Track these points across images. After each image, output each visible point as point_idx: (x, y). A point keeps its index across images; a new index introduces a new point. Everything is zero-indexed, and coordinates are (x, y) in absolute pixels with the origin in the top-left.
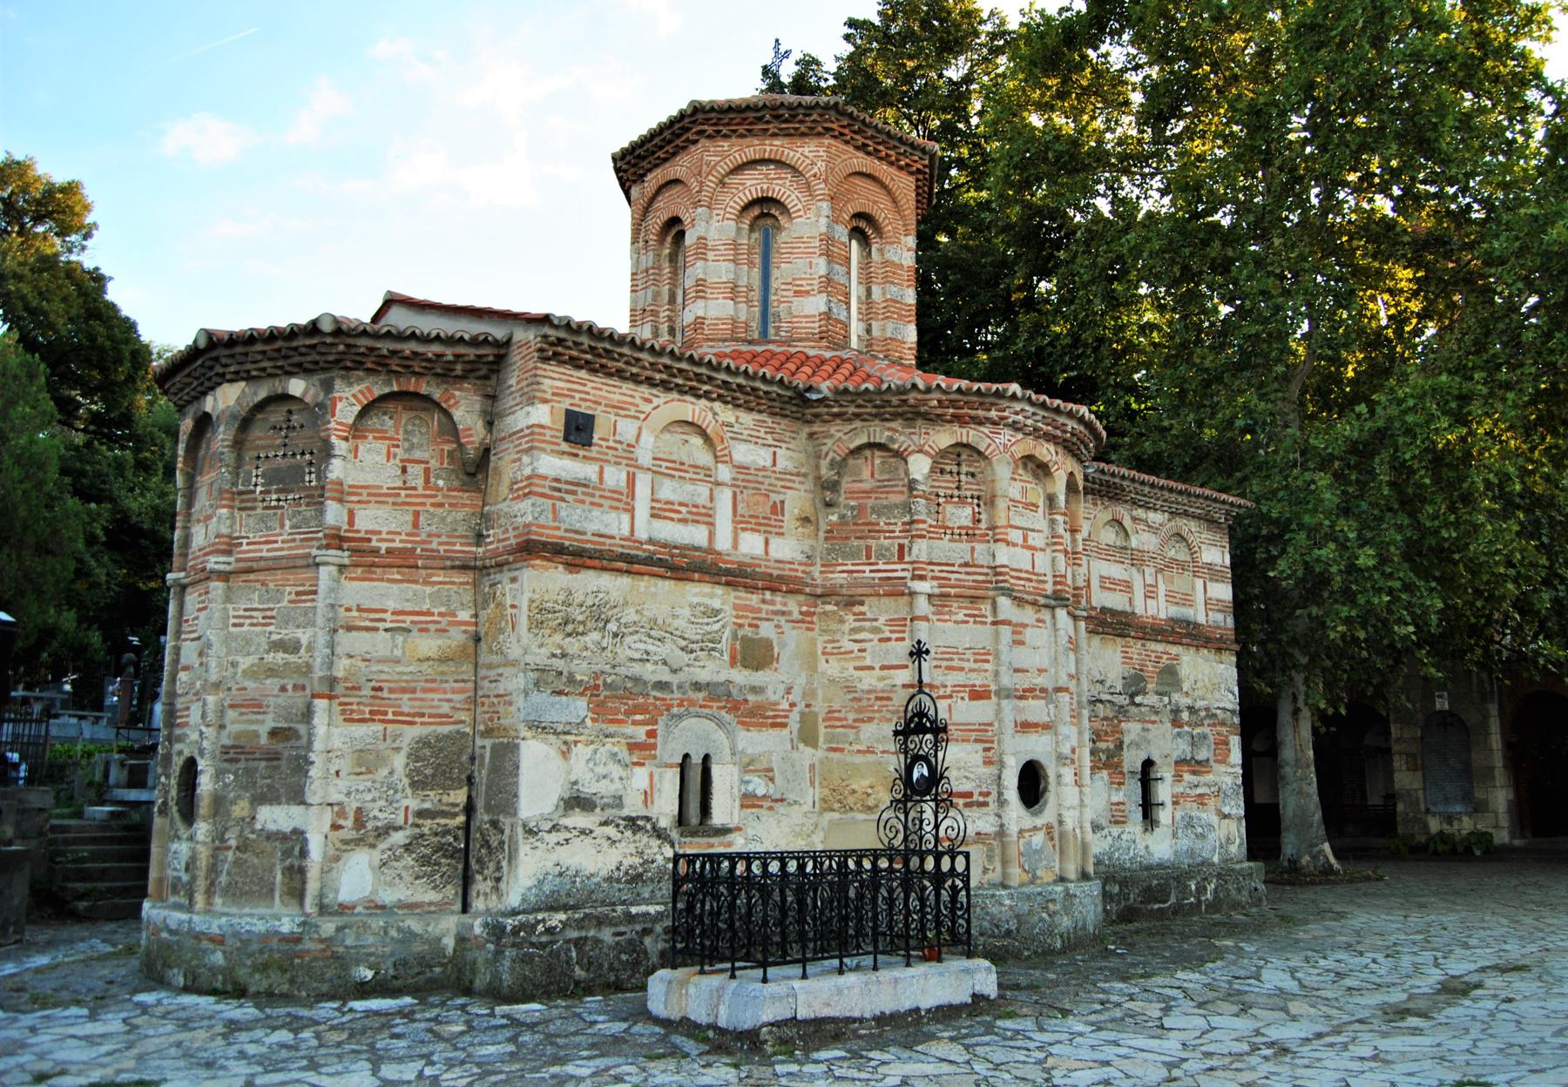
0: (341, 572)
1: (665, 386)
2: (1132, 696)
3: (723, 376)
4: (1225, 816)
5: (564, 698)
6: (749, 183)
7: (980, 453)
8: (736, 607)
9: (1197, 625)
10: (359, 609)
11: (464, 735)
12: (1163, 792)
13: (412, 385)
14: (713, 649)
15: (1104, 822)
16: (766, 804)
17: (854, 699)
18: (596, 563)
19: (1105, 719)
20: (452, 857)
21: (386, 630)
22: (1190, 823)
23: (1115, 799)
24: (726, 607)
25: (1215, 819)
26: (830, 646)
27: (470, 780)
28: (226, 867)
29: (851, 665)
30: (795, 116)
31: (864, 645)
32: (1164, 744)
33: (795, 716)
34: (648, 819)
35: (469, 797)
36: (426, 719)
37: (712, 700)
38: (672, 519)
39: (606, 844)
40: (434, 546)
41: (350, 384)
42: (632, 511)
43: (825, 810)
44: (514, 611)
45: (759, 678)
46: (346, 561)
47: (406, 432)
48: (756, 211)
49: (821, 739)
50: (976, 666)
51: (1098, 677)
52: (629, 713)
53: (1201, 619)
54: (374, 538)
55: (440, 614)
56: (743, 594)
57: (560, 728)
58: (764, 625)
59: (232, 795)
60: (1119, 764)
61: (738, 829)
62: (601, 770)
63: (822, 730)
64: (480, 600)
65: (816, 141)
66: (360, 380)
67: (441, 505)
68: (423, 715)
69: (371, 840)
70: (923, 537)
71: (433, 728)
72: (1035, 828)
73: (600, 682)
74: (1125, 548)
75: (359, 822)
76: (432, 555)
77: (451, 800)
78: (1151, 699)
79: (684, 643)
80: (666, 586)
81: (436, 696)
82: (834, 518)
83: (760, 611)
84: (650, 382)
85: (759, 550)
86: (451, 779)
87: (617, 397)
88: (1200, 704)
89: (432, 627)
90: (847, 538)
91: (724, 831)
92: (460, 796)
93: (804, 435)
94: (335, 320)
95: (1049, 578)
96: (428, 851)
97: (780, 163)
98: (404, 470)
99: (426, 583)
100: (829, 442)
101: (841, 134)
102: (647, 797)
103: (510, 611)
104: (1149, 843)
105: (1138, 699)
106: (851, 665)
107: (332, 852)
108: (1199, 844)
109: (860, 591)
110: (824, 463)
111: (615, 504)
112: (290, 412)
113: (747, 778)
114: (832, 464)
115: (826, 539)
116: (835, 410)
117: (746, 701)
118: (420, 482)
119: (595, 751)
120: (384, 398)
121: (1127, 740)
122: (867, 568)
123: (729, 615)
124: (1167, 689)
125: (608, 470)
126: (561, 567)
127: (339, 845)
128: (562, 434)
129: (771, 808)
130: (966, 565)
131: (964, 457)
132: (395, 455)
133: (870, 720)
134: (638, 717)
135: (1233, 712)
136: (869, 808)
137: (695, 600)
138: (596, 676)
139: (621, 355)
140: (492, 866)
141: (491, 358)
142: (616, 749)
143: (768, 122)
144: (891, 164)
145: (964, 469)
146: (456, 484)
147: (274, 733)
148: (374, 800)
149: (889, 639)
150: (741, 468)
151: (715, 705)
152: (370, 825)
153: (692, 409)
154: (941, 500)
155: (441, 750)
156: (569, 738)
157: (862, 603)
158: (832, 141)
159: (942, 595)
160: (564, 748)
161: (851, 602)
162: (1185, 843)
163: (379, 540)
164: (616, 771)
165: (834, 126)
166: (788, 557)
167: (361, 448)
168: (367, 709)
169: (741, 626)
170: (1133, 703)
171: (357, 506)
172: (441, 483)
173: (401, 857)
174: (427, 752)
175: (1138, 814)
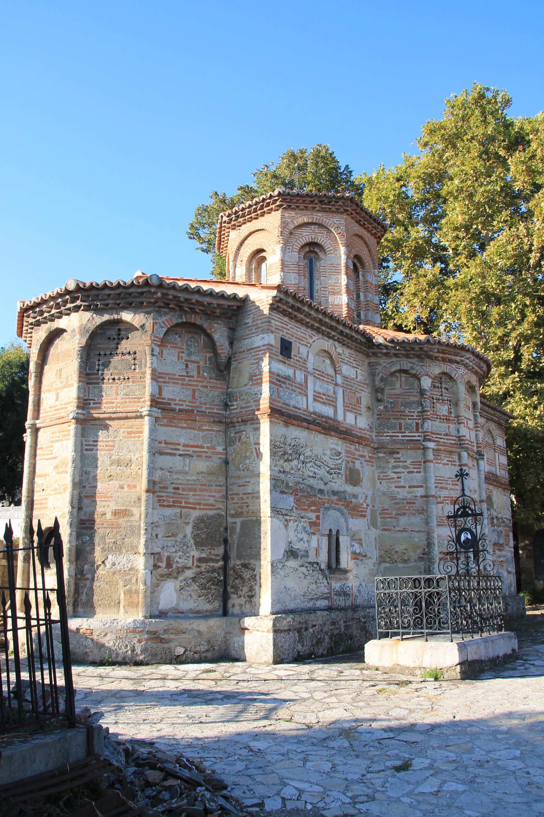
0: (156, 421)
1: (318, 330)
3: (341, 328)
5: (285, 496)
6: (304, 234)
7: (451, 378)
8: (347, 452)
9: (497, 476)
10: (166, 443)
11: (220, 516)
13: (193, 319)
14: (339, 473)
16: (360, 558)
17: (395, 503)
18: (295, 422)
20: (217, 585)
21: (180, 455)
24: (343, 452)
26: (382, 475)
27: (226, 541)
28: (85, 590)
29: (393, 485)
30: (329, 202)
31: (399, 475)
33: (369, 512)
34: (317, 564)
35: (226, 551)
36: (202, 507)
37: (339, 500)
38: (320, 402)
39: (303, 576)
40: (203, 409)
41: (161, 316)
42: (306, 395)
43: (382, 562)
44: (257, 446)
45: (356, 490)
46: (160, 416)
47: (187, 345)
48: (307, 249)
49: (379, 524)
50: (453, 487)
52: (309, 506)
53: (498, 474)
54: (172, 403)
55: (207, 448)
56: (348, 445)
57: (284, 512)
58: (357, 462)
59: (88, 549)
61: (351, 571)
62: (300, 536)
63: (379, 520)
64: (228, 440)
65: (339, 216)
66: (166, 314)
67: (206, 387)
68: (200, 504)
69: (175, 575)
70: (429, 419)
71: (205, 511)
73: (298, 488)
75: (169, 565)
76: (203, 414)
77: (216, 552)
79: (328, 469)
80: (321, 437)
81: (207, 494)
82: (382, 408)
83: (354, 454)
84: (312, 327)
85: (353, 423)
86: (216, 541)
87: (300, 334)
88: (499, 516)
89: (204, 455)
90: (389, 419)
91: (345, 571)
92: (220, 551)
93: (366, 364)
94: (161, 279)
95: (475, 444)
96: (204, 581)
97: (321, 225)
98: (187, 366)
99: (200, 429)
100: (380, 368)
101: (352, 214)
102: (317, 550)
103: (253, 447)
106: (393, 485)
107: (155, 581)
109: (398, 446)
110: (377, 379)
111: (301, 391)
112: (119, 330)
113: (353, 543)
114: (382, 379)
115: (378, 418)
116: (384, 351)
117: (351, 502)
118: (195, 373)
119: (298, 525)
120: (177, 325)
122: (400, 435)
123: (343, 454)
125: (298, 372)
126: (282, 423)
127: (158, 577)
128: (279, 351)
129: (362, 560)
130: (446, 435)
131: (443, 379)
132: (182, 358)
133: (404, 514)
134: (313, 508)
136: (405, 561)
137: (332, 446)
138: (298, 483)
139: (304, 311)
140: (245, 589)
141: (235, 308)
142: (305, 525)
143: (316, 204)
145: (444, 386)
146: (213, 375)
147: (116, 513)
148: (176, 552)
149: (413, 472)
150: (345, 378)
151: (340, 503)
152: (174, 566)
153: (327, 344)
154: (435, 401)
155: (210, 524)
156: (288, 518)
157: (398, 453)
158: (347, 217)
159: (438, 450)
160: (286, 523)
161: (392, 453)
163: (175, 404)
165: (349, 209)
166: (363, 428)
167: (164, 352)
168: (171, 500)
169: (348, 462)
171: (163, 385)
172: (205, 374)
173: (191, 584)
174: (202, 525)
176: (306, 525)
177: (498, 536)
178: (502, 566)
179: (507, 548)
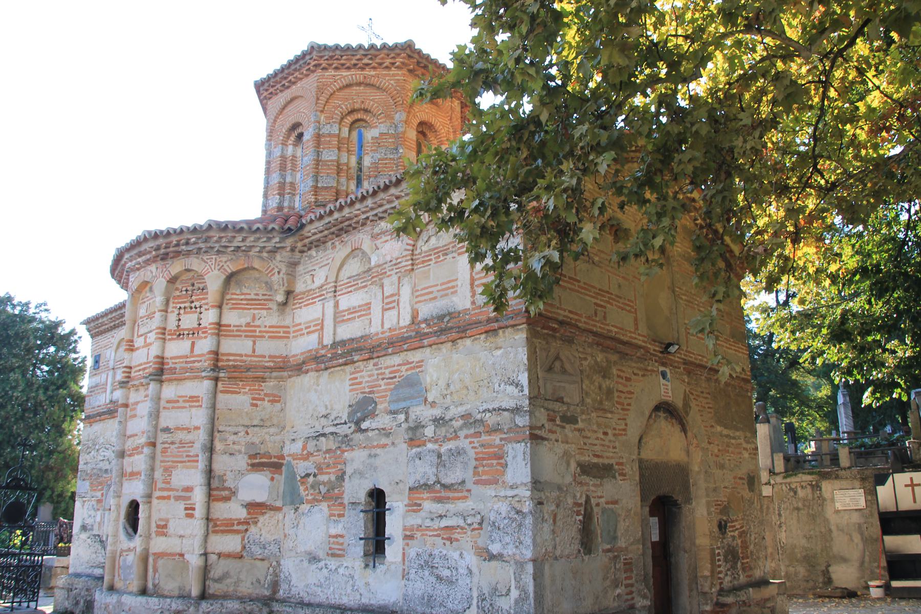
2: (358, 423)
4: (492, 557)
12: (394, 525)
15: (321, 554)
19: (328, 451)
22: (428, 564)
23: (333, 532)
25: (471, 559)
32: (393, 467)
34: (99, 536)
51: (324, 412)
60: (340, 496)
72: (129, 550)
74: (370, 269)
78: (383, 421)
88: (454, 411)
104: (370, 580)
105: (364, 426)
108: (442, 590)
121: (349, 470)
124: (403, 405)
135: (516, 410)
144: (301, 79)
162: (420, 586)
164: (92, 513)
170: (360, 430)
175: (358, 549)
176: (94, 503)
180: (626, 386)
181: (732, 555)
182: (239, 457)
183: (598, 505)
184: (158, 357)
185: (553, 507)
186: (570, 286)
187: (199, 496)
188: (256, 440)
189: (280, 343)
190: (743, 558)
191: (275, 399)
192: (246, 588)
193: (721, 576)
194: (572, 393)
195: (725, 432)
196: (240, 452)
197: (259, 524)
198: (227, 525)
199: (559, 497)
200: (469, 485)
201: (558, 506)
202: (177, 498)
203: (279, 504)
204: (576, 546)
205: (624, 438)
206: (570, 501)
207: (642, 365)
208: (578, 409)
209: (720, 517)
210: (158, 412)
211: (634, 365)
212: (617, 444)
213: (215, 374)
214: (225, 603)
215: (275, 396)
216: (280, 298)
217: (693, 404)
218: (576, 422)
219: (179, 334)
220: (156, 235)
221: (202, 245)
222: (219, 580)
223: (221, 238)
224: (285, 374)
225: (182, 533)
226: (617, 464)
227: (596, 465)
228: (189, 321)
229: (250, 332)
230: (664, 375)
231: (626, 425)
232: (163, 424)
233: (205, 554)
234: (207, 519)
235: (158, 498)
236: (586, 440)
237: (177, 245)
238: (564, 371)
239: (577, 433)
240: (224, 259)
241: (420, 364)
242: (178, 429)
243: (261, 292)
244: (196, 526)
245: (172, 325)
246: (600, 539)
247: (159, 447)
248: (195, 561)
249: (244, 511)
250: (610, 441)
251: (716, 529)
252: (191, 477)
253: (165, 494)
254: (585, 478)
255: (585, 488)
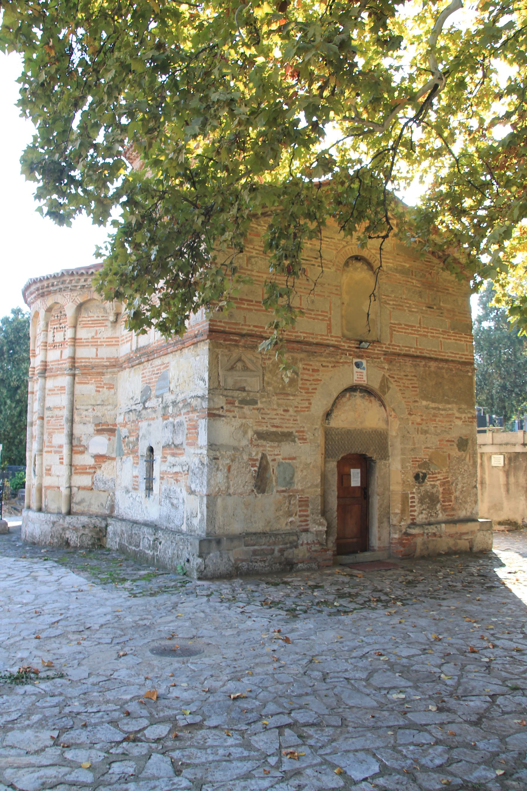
15: (130, 488)
60: (137, 451)
108: (173, 512)
121: (141, 435)
135: (202, 398)
162: (166, 509)
170: (145, 408)
177: (174, 432)
178: (177, 480)
179: (191, 450)
180: (313, 376)
181: (430, 500)
182: (89, 425)
183: (274, 460)
184: (42, 361)
185: (228, 461)
186: (256, 308)
187: (65, 451)
188: (99, 414)
189: (113, 349)
190: (444, 501)
191: (111, 387)
192: (95, 509)
193: (416, 514)
194: (253, 383)
195: (433, 405)
196: (89, 422)
197: (102, 469)
198: (83, 469)
199: (234, 455)
200: (184, 446)
201: (232, 461)
202: (56, 452)
203: (114, 455)
204: (250, 487)
205: (306, 413)
206: (245, 457)
207: (333, 359)
208: (258, 395)
209: (417, 470)
210: (44, 397)
211: (323, 359)
212: (298, 418)
213: (72, 372)
214: (79, 517)
215: (110, 384)
216: (112, 318)
217: (393, 386)
218: (256, 403)
219: (54, 346)
220: (35, 282)
221: (61, 286)
222: (79, 504)
223: (71, 281)
224: (116, 370)
225: (58, 474)
226: (297, 432)
227: (275, 434)
228: (59, 337)
229: (94, 343)
230: (358, 365)
231: (310, 404)
232: (47, 405)
233: (70, 487)
234: (71, 465)
235: (47, 452)
236: (264, 416)
237: (48, 287)
238: (245, 368)
239: (256, 411)
240: (75, 294)
241: (167, 366)
242: (55, 408)
243: (101, 315)
244: (63, 470)
245: (50, 340)
246: (274, 483)
247: (46, 419)
248: (64, 491)
249: (93, 460)
250: (291, 416)
251: (411, 479)
252: (61, 439)
253: (49, 449)
254: (261, 442)
255: (261, 449)
